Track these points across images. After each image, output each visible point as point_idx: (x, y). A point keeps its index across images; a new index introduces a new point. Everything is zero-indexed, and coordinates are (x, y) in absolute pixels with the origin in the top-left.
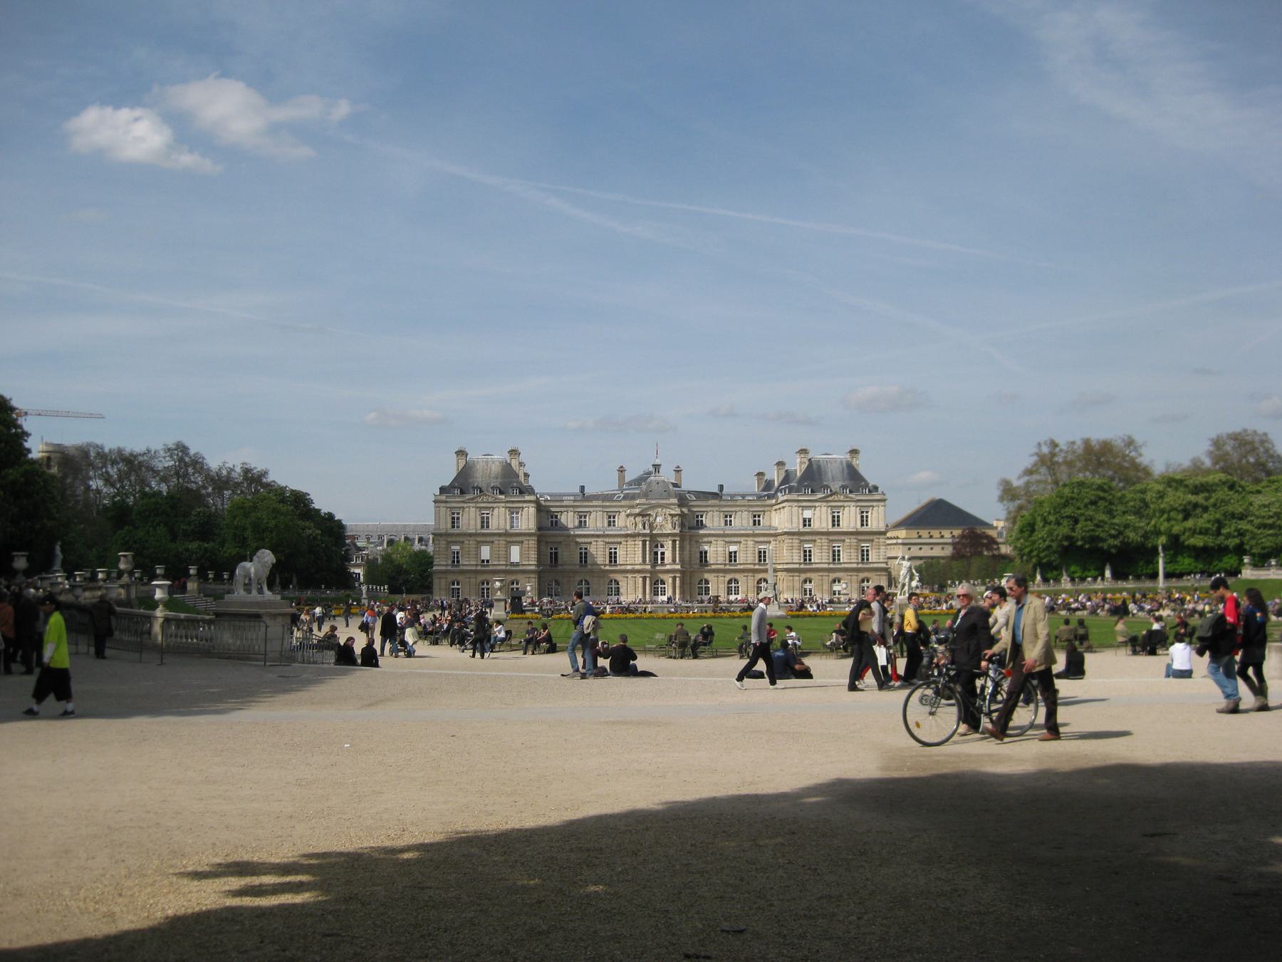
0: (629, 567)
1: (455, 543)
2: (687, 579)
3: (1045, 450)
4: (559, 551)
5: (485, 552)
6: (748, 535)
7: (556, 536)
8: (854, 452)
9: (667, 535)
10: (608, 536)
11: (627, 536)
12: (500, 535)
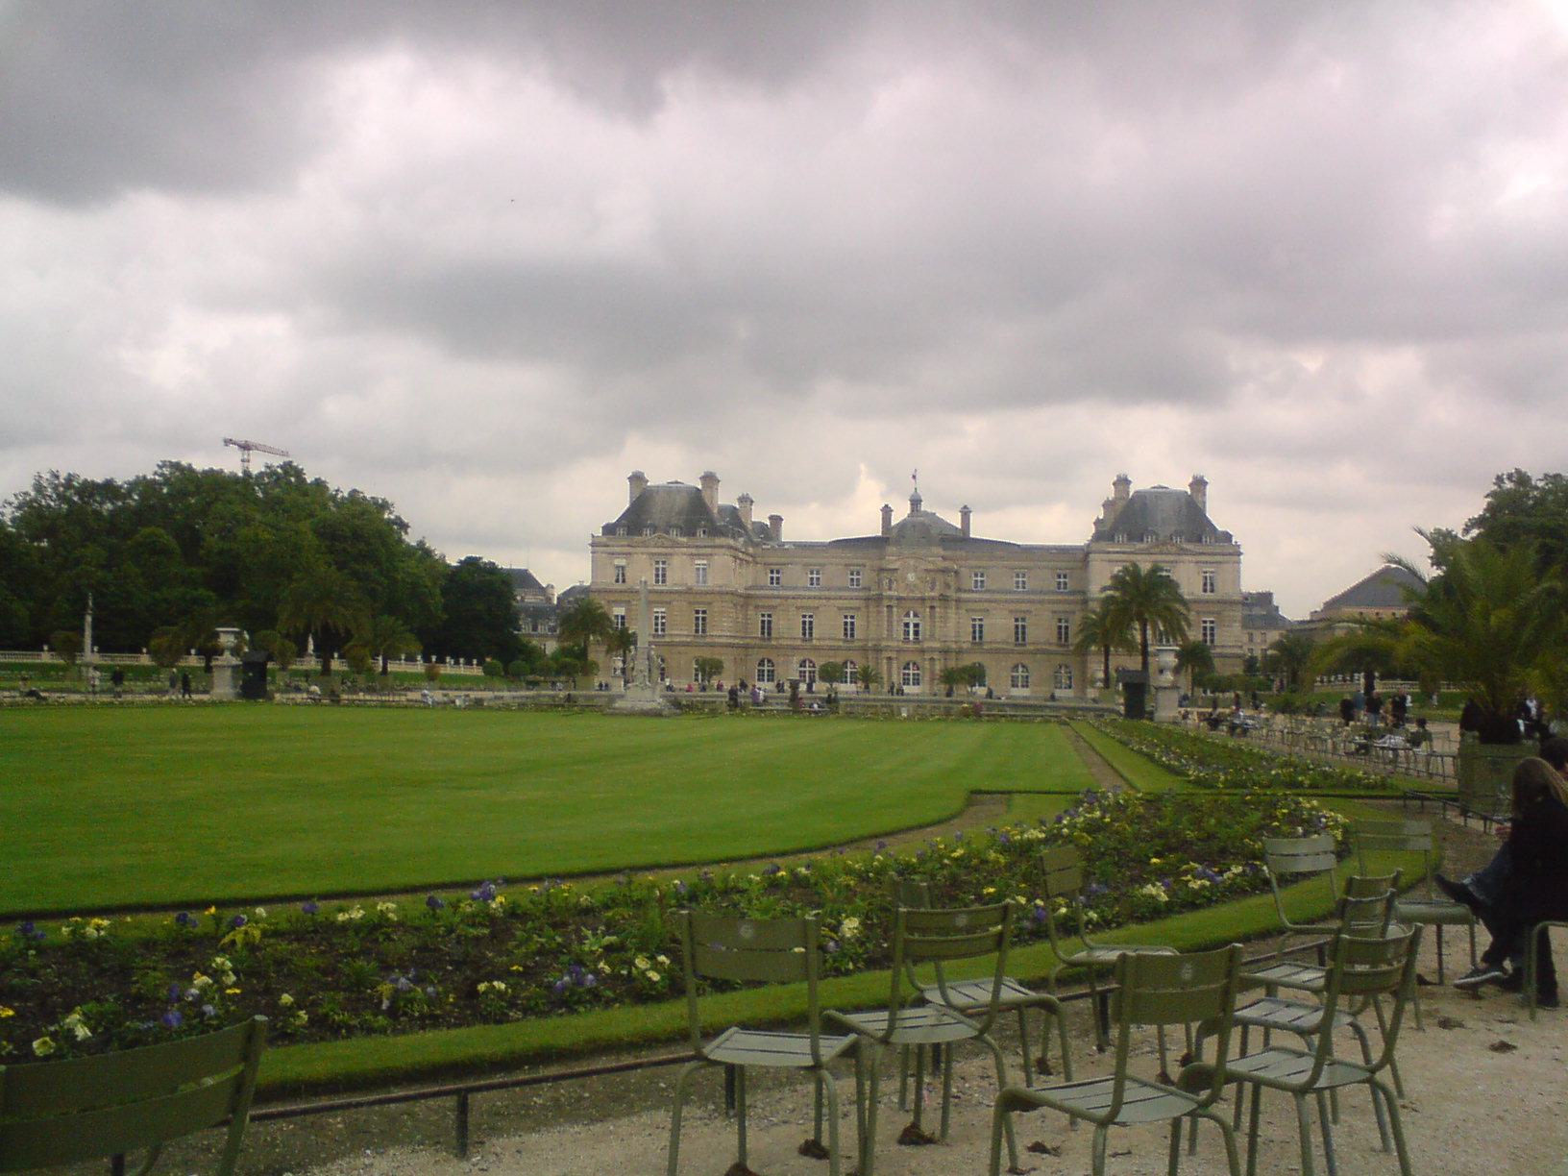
3: (1508, 485)
4: (774, 619)
9: (923, 599)
11: (867, 599)
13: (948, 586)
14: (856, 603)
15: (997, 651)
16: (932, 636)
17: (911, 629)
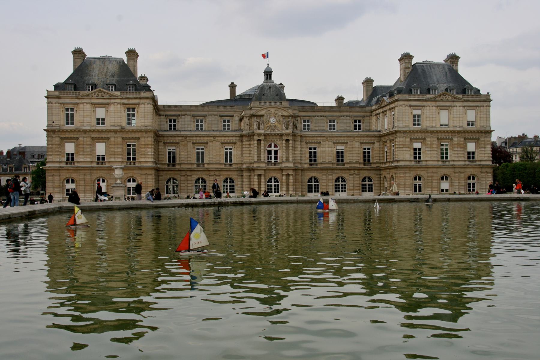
0: (244, 166)
1: (69, 139)
2: (299, 177)
4: (177, 152)
5: (101, 149)
6: (354, 137)
7: (173, 136)
8: (454, 59)
9: (281, 135)
10: (223, 136)
11: (242, 136)
12: (115, 132)
13: (295, 126)
14: (234, 139)
15: (327, 169)
16: (287, 160)
17: (273, 155)
